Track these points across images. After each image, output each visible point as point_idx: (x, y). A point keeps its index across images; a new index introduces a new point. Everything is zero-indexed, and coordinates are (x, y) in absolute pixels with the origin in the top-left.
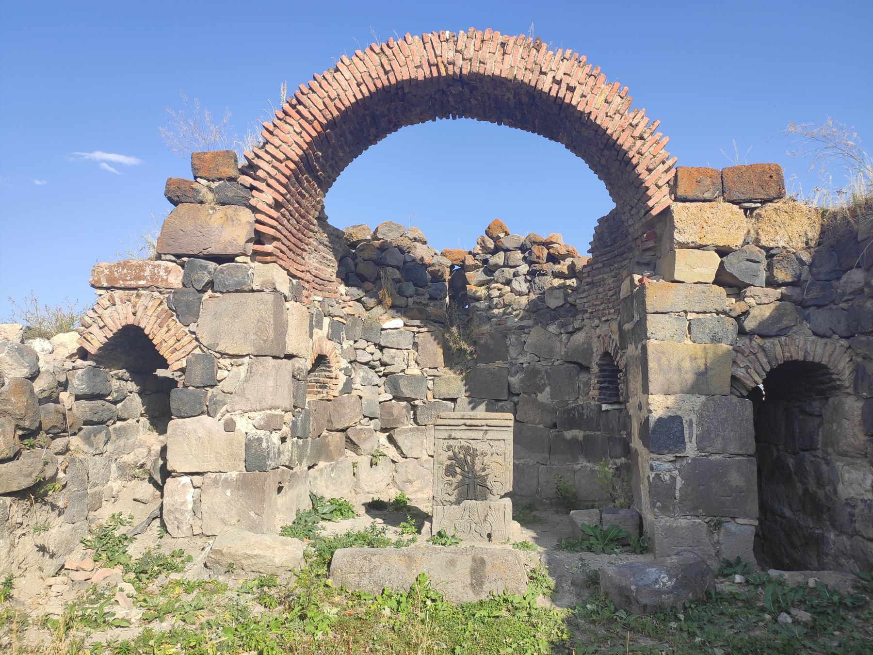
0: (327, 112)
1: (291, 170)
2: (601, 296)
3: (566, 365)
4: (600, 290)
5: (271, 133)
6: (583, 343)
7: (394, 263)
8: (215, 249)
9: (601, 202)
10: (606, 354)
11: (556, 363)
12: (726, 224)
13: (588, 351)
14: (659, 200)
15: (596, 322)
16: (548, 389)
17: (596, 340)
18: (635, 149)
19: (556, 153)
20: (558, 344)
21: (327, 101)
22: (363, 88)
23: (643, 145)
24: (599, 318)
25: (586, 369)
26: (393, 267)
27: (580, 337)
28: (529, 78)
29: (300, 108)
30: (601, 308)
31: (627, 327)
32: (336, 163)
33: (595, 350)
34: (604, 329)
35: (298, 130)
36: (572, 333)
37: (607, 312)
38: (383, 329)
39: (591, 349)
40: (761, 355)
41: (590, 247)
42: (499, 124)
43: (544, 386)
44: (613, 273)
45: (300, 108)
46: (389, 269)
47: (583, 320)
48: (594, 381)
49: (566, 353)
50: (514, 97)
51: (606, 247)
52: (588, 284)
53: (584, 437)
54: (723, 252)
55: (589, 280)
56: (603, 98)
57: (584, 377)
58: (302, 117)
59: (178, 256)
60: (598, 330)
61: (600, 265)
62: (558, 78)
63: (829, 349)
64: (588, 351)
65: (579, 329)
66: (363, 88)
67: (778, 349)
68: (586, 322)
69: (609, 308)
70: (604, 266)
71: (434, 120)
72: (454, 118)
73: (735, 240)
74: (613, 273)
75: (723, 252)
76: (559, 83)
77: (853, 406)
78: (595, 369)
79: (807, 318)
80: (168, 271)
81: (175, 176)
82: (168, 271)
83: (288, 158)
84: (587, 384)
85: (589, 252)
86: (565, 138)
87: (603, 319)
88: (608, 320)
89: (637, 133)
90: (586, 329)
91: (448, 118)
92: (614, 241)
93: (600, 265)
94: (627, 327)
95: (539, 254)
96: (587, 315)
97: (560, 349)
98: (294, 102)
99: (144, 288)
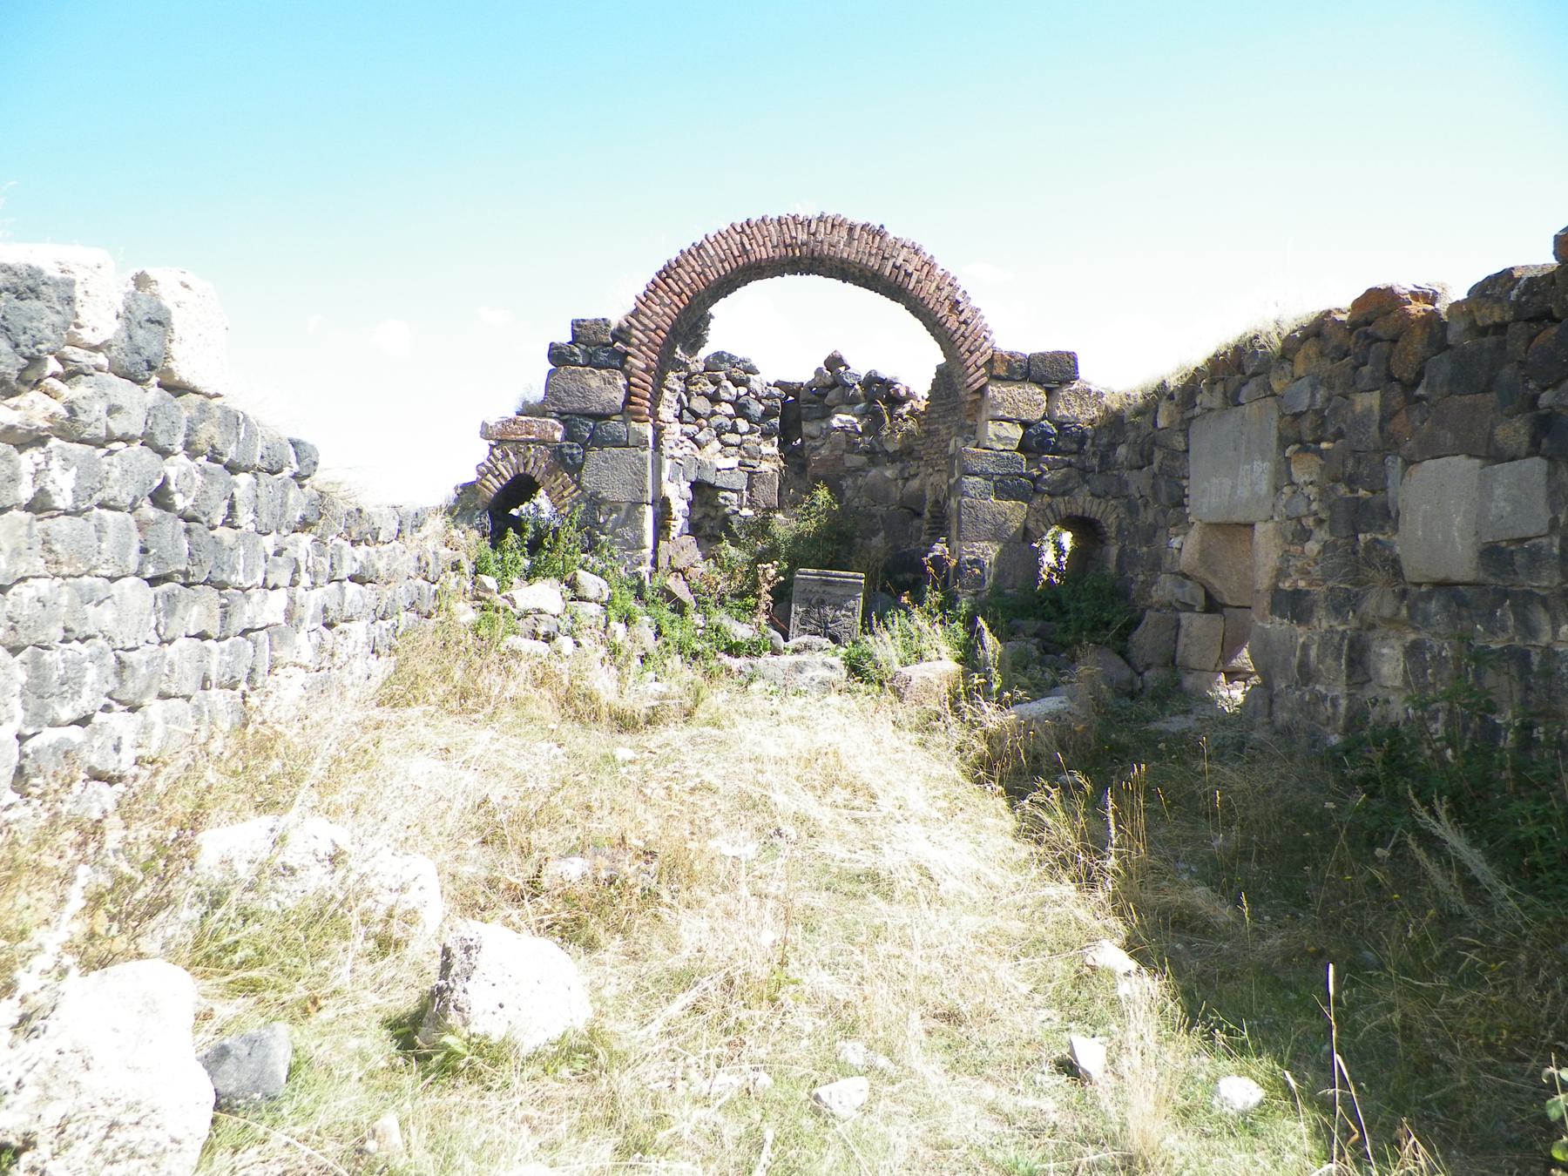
7: (727, 397)
8: (596, 408)
9: (934, 356)
10: (937, 502)
12: (1028, 400)
13: (920, 498)
14: (978, 378)
16: (882, 534)
19: (900, 307)
22: (726, 265)
25: (919, 515)
28: (874, 263)
31: (952, 481)
35: (668, 301)
36: (907, 479)
40: (1048, 512)
43: (879, 530)
45: (669, 281)
54: (1026, 425)
57: (916, 522)
58: (671, 290)
59: (561, 414)
63: (1103, 506)
64: (920, 498)
65: (916, 475)
66: (726, 265)
67: (1062, 507)
73: (1036, 415)
75: (1026, 425)
77: (1114, 551)
78: (927, 515)
79: (1087, 482)
80: (554, 428)
81: (557, 341)
82: (554, 428)
83: (658, 327)
84: (919, 530)
89: (962, 319)
94: (952, 481)
95: (881, 392)
97: (896, 494)
99: (533, 441)
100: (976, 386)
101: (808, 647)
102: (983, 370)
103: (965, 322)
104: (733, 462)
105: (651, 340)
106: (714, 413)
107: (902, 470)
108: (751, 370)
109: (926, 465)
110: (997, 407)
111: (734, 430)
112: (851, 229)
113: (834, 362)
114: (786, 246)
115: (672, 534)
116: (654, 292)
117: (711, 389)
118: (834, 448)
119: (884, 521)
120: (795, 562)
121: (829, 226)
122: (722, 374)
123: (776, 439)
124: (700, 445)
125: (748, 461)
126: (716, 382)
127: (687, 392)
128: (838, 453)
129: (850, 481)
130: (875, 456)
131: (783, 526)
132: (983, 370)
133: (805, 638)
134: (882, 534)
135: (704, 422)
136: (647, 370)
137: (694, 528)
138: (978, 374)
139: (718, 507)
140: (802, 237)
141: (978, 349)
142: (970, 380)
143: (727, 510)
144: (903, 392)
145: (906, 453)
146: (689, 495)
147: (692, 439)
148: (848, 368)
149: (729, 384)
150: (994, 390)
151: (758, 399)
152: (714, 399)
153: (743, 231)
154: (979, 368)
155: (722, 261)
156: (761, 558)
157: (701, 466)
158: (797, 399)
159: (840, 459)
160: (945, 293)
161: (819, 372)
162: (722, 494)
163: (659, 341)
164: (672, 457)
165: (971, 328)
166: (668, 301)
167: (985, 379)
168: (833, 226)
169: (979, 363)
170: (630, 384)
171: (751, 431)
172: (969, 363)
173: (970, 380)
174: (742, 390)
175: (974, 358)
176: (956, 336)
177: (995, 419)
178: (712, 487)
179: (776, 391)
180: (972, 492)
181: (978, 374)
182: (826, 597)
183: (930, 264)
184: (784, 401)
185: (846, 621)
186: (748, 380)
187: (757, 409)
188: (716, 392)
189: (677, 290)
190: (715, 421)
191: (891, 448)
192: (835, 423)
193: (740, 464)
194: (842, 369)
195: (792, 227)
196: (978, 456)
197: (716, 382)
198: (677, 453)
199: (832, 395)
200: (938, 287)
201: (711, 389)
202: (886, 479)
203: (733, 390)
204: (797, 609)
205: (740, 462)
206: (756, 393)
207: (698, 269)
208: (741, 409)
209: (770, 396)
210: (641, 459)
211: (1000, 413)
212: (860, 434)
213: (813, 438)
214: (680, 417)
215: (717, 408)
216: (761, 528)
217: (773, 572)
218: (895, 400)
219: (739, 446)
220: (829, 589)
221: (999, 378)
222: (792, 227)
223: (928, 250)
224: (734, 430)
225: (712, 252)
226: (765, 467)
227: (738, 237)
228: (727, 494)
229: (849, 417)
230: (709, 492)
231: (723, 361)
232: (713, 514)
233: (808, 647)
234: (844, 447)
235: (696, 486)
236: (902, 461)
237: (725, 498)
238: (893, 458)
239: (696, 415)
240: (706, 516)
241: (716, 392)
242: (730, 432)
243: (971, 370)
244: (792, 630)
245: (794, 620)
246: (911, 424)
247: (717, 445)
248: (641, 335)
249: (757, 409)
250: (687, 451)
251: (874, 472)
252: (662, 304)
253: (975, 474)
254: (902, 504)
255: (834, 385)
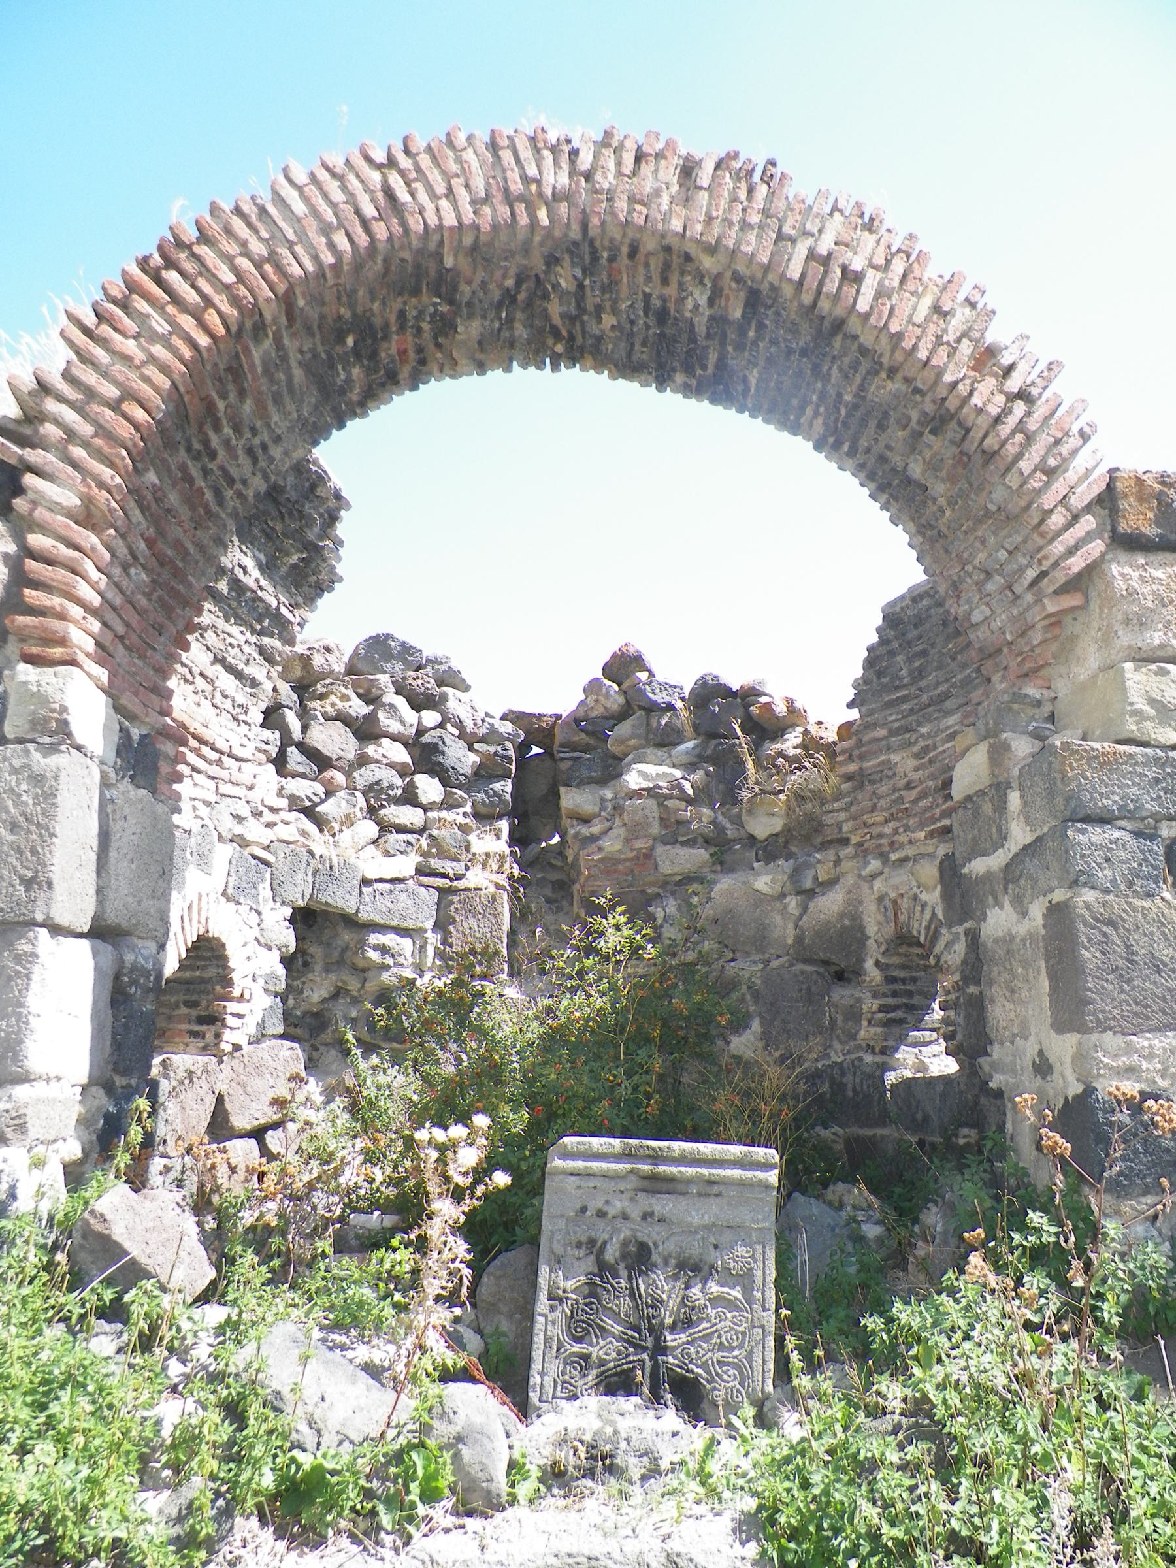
0: (243, 291)
1: (137, 427)
2: (883, 803)
3: (800, 966)
4: (883, 789)
5: (87, 332)
6: (842, 916)
7: (394, 727)
10: (903, 939)
11: (775, 963)
15: (875, 865)
16: (756, 1026)
17: (873, 907)
18: (1011, 421)
20: (778, 919)
21: (244, 263)
23: (1028, 414)
24: (884, 857)
26: (394, 738)
27: (830, 904)
29: (172, 276)
30: (887, 830)
32: (264, 447)
33: (872, 930)
34: (895, 882)
36: (810, 894)
37: (902, 838)
38: (366, 882)
39: (862, 929)
41: (850, 694)
42: (661, 388)
44: (915, 749)
45: (172, 276)
46: (385, 741)
47: (838, 862)
48: (870, 1004)
49: (799, 939)
50: (711, 302)
51: (897, 688)
52: (848, 778)
53: (848, 1142)
55: (852, 767)
56: (926, 303)
57: (841, 995)
58: (176, 299)
60: (878, 884)
61: (881, 732)
62: (823, 250)
68: (846, 865)
69: (907, 828)
70: (892, 733)
71: (508, 369)
72: (555, 367)
74: (915, 749)
76: (826, 261)
83: (128, 395)
84: (853, 1014)
85: (850, 705)
86: (819, 423)
87: (893, 857)
88: (906, 859)
89: (1014, 384)
90: (850, 880)
91: (540, 366)
92: (920, 674)
93: (881, 732)
96: (849, 850)
98: (157, 260)
100: (1076, 564)
101: (601, 1462)
102: (1088, 522)
103: (1023, 395)
104: (405, 865)
105: (102, 430)
106: (363, 760)
107: (795, 875)
108: (451, 679)
109: (862, 852)
110: (1141, 623)
111: (410, 798)
112: (688, 170)
113: (623, 666)
114: (510, 199)
115: (229, 1037)
116: (124, 305)
117: (358, 708)
118: (635, 830)
119: (756, 996)
120: (551, 1116)
121: (629, 159)
122: (384, 679)
123: (504, 825)
124: (321, 822)
125: (435, 863)
126: (371, 698)
127: (304, 715)
128: (640, 844)
129: (672, 906)
130: (724, 850)
131: (512, 1011)
132: (1088, 522)
133: (586, 1416)
134: (756, 1026)
135: (339, 778)
136: (87, 517)
137: (306, 1026)
138: (1079, 530)
139: (364, 971)
140: (556, 178)
141: (1065, 463)
142: (1058, 548)
143: (386, 977)
144: (781, 709)
145: (806, 835)
146: (288, 938)
147: (309, 812)
148: (651, 674)
149: (401, 702)
150: (1125, 572)
151: (470, 740)
152: (366, 731)
153: (392, 162)
154: (1076, 518)
155: (326, 230)
156: (448, 1106)
157: (324, 872)
158: (549, 753)
159: (648, 855)
160: (956, 324)
161: (592, 687)
162: (374, 938)
163: (125, 431)
164: (242, 842)
165: (1040, 411)
166: (160, 325)
167: (1097, 547)
168: (639, 157)
169: (1077, 502)
170: (28, 552)
171: (448, 804)
172: (1048, 500)
173: (1058, 548)
174: (430, 718)
175: (1059, 487)
176: (1004, 430)
177: (1143, 658)
178: (350, 921)
179: (507, 728)
180: (1105, 875)
181: (1079, 530)
182: (650, 1233)
183: (911, 255)
184: (522, 748)
185: (726, 1323)
186: (444, 698)
187: (461, 758)
188: (371, 718)
189: (191, 297)
190: (364, 776)
191: (763, 826)
192: (633, 779)
193: (420, 871)
194: (643, 676)
195: (526, 154)
196: (1105, 762)
197: (371, 698)
198: (254, 831)
199: (624, 728)
200: (937, 309)
201: (358, 708)
202: (759, 899)
203: (410, 716)
204: (559, 1281)
205: (417, 877)
206: (460, 725)
207: (258, 249)
208: (425, 755)
209: (492, 736)
210: (37, 779)
211: (1157, 638)
212: (690, 801)
213: (586, 821)
214: (280, 762)
215: (371, 750)
216: (459, 1008)
217: (469, 1157)
218: (765, 727)
219: (420, 832)
220: (662, 1205)
221: (1132, 543)
222: (526, 154)
223: (898, 223)
224: (410, 798)
225: (299, 208)
226: (475, 878)
227: (375, 177)
228: (389, 939)
229: (664, 769)
230: (347, 936)
231: (388, 656)
232: (353, 985)
233: (601, 1462)
234: (656, 829)
235: (306, 919)
236: (789, 856)
237: (384, 950)
238: (770, 850)
239: (320, 761)
240: (338, 993)
241: (371, 718)
242: (398, 801)
243: (1057, 520)
244: (544, 1371)
245: (548, 1323)
246: (809, 777)
247: (370, 829)
248: (70, 416)
249: (461, 758)
250: (283, 832)
251: (725, 884)
252: (145, 334)
253: (1104, 819)
254: (802, 951)
255: (624, 714)
